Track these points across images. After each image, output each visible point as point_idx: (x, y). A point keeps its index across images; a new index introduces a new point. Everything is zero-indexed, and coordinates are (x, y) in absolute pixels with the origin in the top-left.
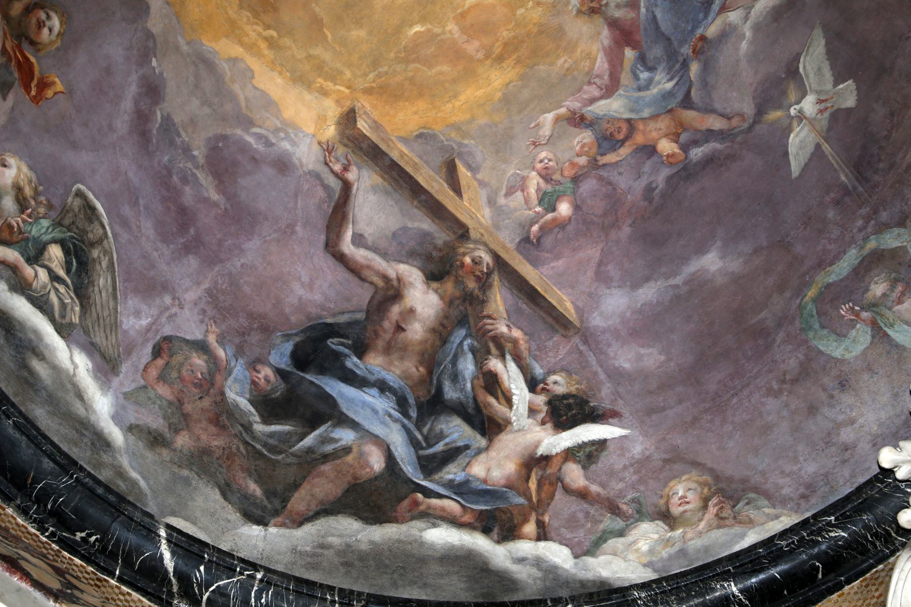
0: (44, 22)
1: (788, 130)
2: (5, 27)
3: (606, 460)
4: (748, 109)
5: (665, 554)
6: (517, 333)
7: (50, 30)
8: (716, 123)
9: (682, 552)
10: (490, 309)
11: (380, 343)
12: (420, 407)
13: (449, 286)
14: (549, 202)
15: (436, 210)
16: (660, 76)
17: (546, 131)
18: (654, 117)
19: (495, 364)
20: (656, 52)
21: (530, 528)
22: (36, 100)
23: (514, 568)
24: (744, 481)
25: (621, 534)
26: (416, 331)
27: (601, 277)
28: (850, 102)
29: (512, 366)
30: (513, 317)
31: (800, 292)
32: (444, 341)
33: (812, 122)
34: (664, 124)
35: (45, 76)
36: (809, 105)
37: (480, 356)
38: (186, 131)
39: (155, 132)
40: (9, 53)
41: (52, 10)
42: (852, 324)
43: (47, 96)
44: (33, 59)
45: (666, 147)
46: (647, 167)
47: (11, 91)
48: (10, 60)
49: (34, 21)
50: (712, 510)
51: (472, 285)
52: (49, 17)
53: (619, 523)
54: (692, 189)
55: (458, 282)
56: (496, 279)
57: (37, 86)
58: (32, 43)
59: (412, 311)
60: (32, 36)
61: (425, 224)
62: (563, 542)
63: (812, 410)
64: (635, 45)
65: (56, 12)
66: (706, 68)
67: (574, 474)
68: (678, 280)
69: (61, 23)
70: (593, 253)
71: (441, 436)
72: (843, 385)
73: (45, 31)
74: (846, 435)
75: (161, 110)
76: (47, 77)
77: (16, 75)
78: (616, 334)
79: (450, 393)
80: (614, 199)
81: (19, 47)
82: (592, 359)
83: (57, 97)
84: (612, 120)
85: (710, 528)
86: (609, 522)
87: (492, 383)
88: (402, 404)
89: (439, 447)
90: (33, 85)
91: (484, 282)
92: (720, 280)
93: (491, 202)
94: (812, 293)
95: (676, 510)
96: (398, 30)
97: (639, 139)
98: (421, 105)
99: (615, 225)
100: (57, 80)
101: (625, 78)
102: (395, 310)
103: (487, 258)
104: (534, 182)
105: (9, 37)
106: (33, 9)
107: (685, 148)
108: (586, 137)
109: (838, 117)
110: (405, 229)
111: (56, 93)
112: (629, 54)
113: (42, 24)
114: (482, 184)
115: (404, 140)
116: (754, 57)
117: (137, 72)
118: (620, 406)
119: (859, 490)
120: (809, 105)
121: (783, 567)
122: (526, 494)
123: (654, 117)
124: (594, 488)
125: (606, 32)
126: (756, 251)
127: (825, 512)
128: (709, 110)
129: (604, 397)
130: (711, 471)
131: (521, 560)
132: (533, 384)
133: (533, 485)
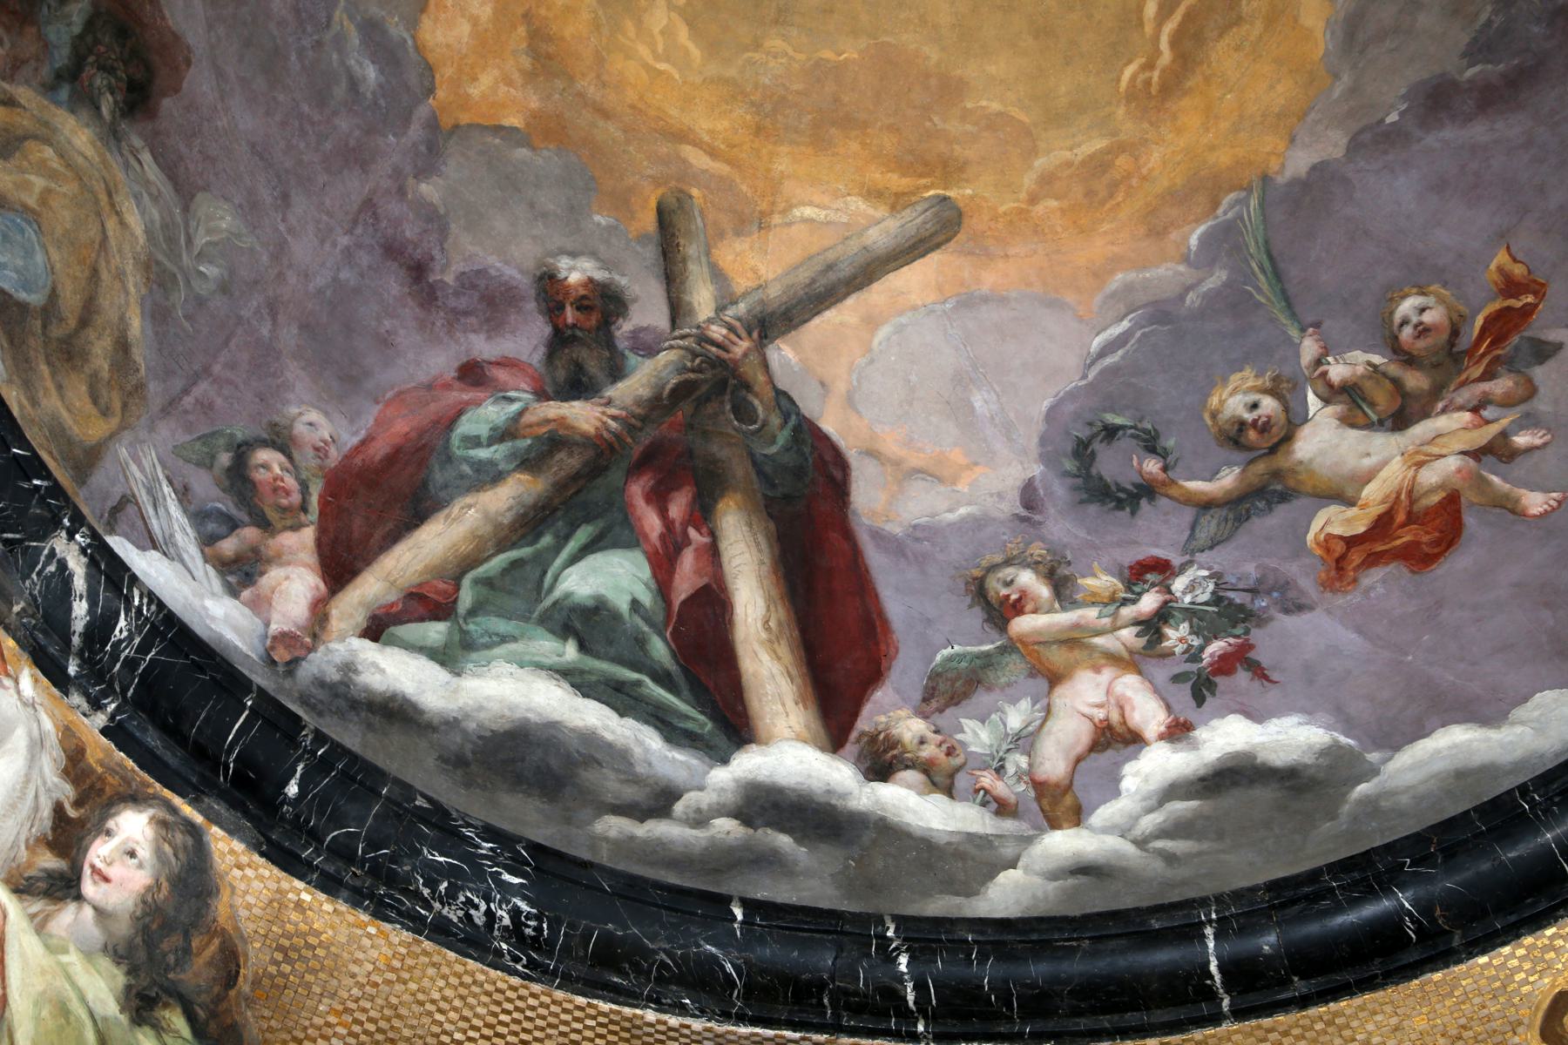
0: (1416, 326)
2: (1452, 388)
7: (1422, 310)
22: (1539, 290)
35: (1495, 289)
38: (1477, 15)
39: (1501, 67)
40: (1487, 365)
41: (1392, 321)
43: (1526, 273)
44: (1479, 321)
47: (1543, 338)
48: (1498, 358)
49: (1421, 344)
52: (1405, 322)
57: (1516, 296)
58: (1455, 333)
60: (1445, 336)
65: (1392, 313)
69: (1404, 297)
73: (1427, 318)
75: (1461, 72)
76: (1496, 283)
77: (1515, 339)
81: (1470, 352)
83: (1520, 256)
90: (1518, 304)
100: (1493, 266)
105: (1464, 377)
106: (1406, 353)
111: (1515, 260)
113: (1421, 328)
117: (1420, 140)
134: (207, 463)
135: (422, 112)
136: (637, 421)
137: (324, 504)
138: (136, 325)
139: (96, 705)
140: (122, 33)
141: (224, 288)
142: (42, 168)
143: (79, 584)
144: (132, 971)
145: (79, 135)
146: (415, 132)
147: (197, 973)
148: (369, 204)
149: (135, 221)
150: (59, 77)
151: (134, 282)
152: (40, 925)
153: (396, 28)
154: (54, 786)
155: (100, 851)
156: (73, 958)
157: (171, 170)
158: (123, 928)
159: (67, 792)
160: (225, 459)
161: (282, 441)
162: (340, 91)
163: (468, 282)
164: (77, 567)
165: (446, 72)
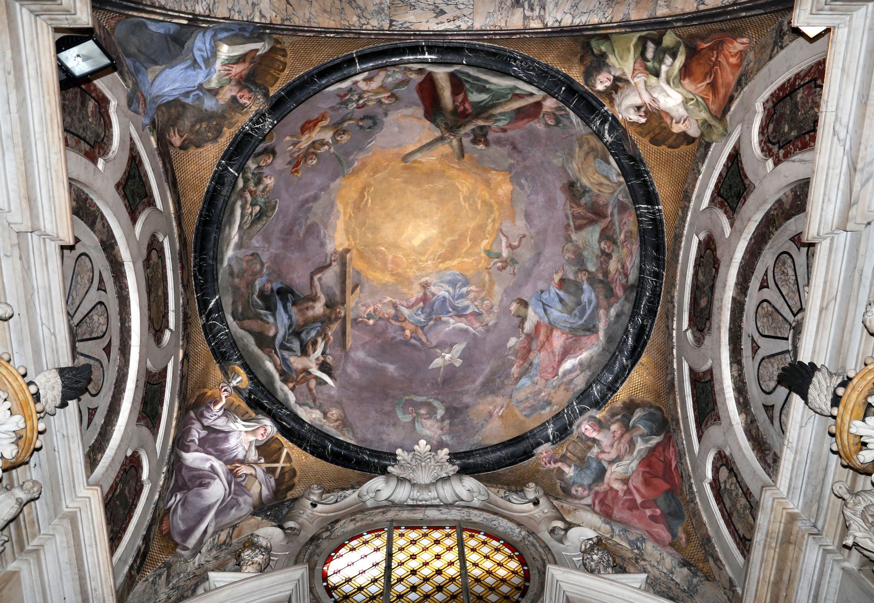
1: (437, 357)
3: (323, 388)
4: (434, 343)
5: (317, 422)
6: (332, 338)
8: (424, 339)
9: (322, 426)
10: (331, 326)
11: (300, 307)
12: (294, 331)
13: (328, 311)
14: (369, 317)
15: (343, 291)
16: (423, 316)
17: (385, 301)
18: (412, 323)
19: (320, 340)
20: (427, 310)
21: (291, 385)
23: (279, 390)
24: (351, 424)
25: (311, 408)
26: (310, 313)
27: (363, 345)
28: (457, 365)
29: (323, 344)
30: (334, 334)
31: (405, 395)
32: (314, 322)
33: (445, 360)
34: (412, 327)
36: (448, 356)
37: (319, 334)
42: (409, 413)
45: (408, 332)
46: (399, 332)
50: (337, 423)
51: (333, 316)
53: (312, 405)
54: (403, 348)
55: (331, 312)
56: (340, 321)
59: (314, 308)
61: (337, 292)
62: (296, 396)
63: (382, 424)
64: (424, 304)
66: (434, 325)
67: (313, 383)
68: (380, 364)
70: (367, 338)
71: (291, 343)
72: (394, 425)
74: (384, 437)
78: (354, 362)
79: (303, 335)
80: (384, 331)
82: (343, 361)
84: (402, 314)
85: (333, 427)
86: (310, 402)
87: (315, 343)
88: (290, 326)
89: (289, 345)
91: (336, 319)
92: (389, 374)
93: (357, 303)
94: (407, 398)
95: (329, 415)
96: (379, 244)
97: (404, 324)
98: (365, 265)
99: (378, 337)
101: (415, 308)
102: (311, 303)
103: (343, 314)
104: (371, 309)
107: (412, 337)
108: (393, 311)
109: (451, 365)
110: (332, 288)
112: (421, 304)
114: (359, 297)
115: (353, 269)
116: (447, 334)
118: (338, 379)
119: (381, 452)
120: (448, 356)
121: (346, 452)
122: (297, 376)
123: (412, 323)
124: (314, 391)
125: (421, 294)
126: (403, 376)
127: (368, 450)
128: (425, 335)
129: (337, 373)
130: (345, 415)
131: (282, 390)
132: (323, 353)
133: (301, 376)
134: (564, 125)
135: (513, 174)
136: (470, 121)
137: (539, 113)
138: (577, 149)
139: (606, 111)
140: (574, 195)
141: (557, 151)
142: (594, 179)
143: (606, 132)
144: (604, 62)
145: (585, 181)
146: (514, 171)
147: (589, 59)
148: (524, 160)
149: (575, 165)
150: (588, 192)
151: (577, 156)
152: (624, 73)
153: (517, 188)
154: (617, 98)
155: (608, 84)
156: (618, 66)
157: (566, 171)
158: (605, 69)
159: (614, 96)
160: (561, 125)
161: (547, 125)
162: (529, 179)
163: (505, 146)
164: (607, 135)
165: (508, 180)
